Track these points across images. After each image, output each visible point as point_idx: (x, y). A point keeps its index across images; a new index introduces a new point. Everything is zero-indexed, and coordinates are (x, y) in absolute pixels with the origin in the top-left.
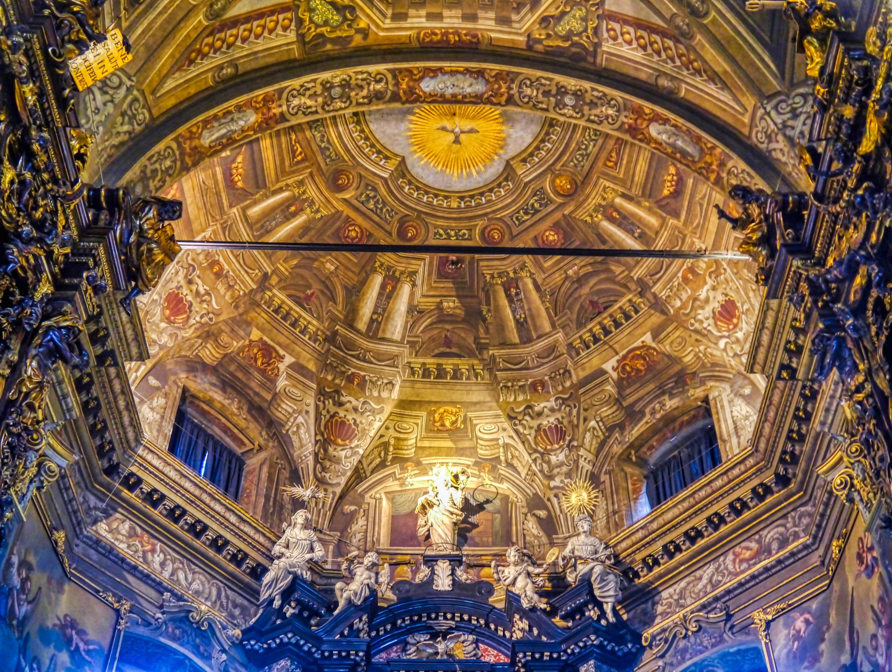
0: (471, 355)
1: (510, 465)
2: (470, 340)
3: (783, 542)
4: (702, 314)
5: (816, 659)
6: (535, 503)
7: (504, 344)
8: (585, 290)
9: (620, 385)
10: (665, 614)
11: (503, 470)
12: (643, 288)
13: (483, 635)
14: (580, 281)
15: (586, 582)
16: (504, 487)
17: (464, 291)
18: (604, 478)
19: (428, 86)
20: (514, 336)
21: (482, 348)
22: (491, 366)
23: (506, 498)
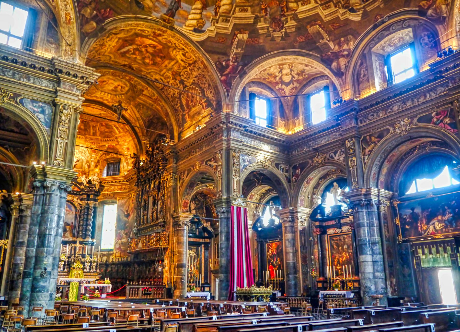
0: (83, 135)
1: (84, 154)
2: (84, 133)
3: (125, 189)
4: (124, 147)
5: (123, 207)
6: (88, 162)
7: (89, 135)
8: (107, 134)
9: (107, 148)
10: (105, 191)
11: (83, 154)
12: (116, 138)
13: (76, 185)
14: (106, 132)
15: (95, 185)
16: (83, 158)
17: (85, 126)
18: (100, 162)
19: (92, 106)
20: (92, 134)
21: (85, 135)
22: (86, 138)
23: (83, 160)
